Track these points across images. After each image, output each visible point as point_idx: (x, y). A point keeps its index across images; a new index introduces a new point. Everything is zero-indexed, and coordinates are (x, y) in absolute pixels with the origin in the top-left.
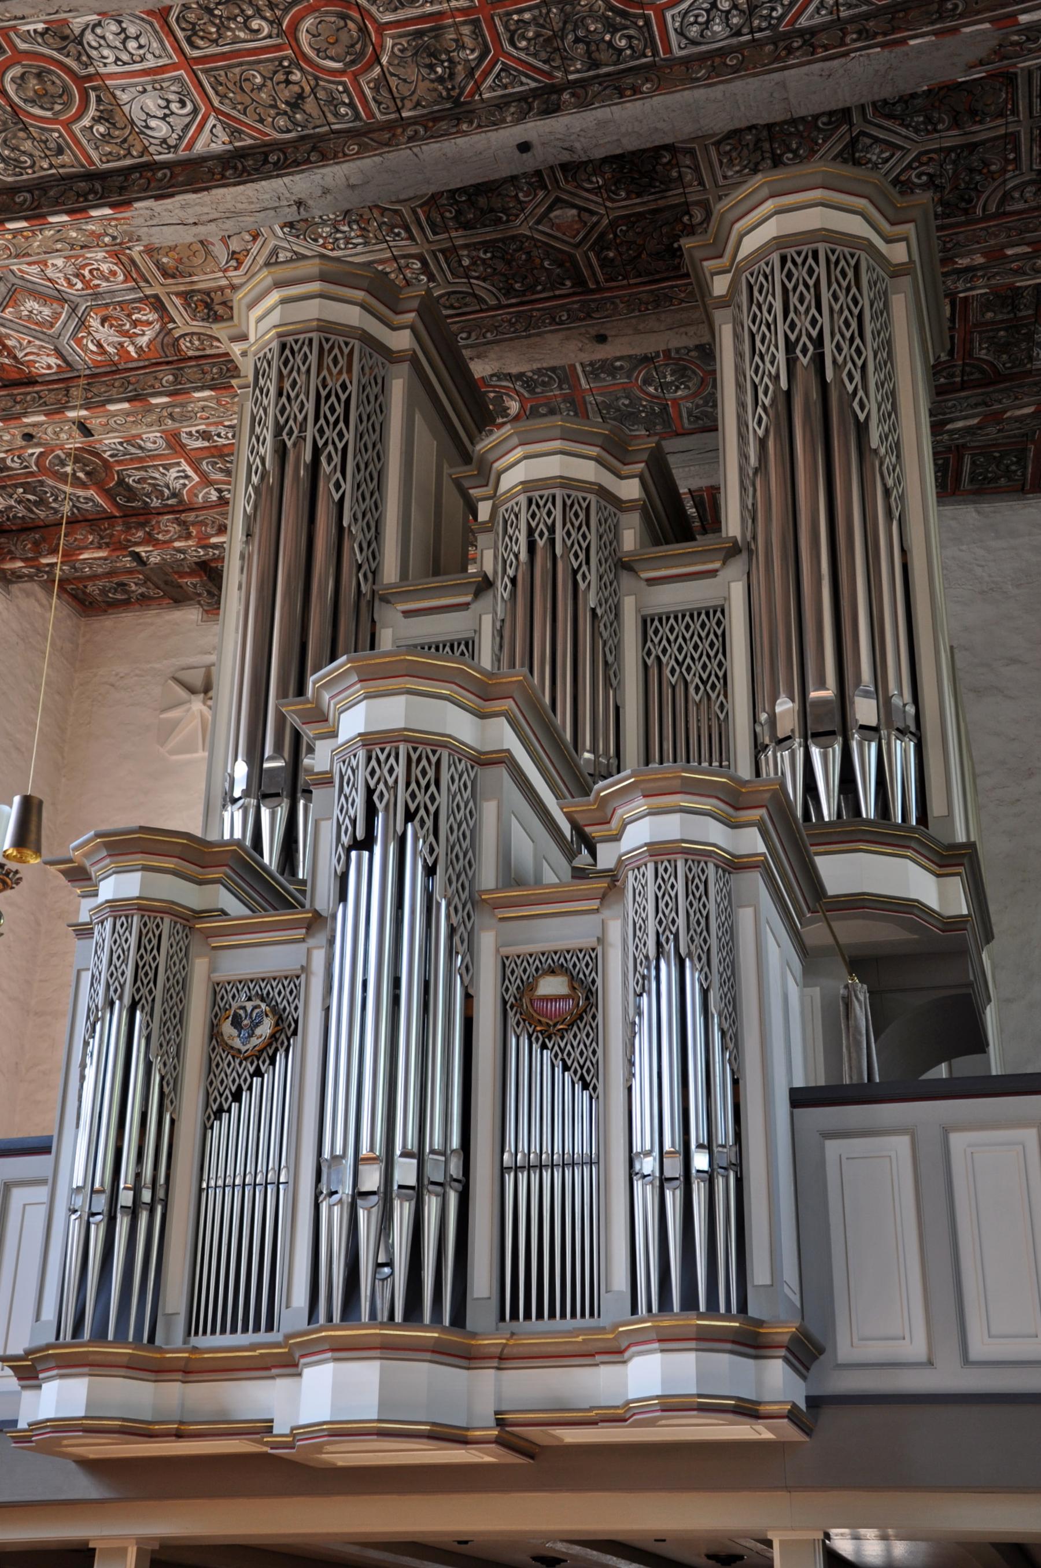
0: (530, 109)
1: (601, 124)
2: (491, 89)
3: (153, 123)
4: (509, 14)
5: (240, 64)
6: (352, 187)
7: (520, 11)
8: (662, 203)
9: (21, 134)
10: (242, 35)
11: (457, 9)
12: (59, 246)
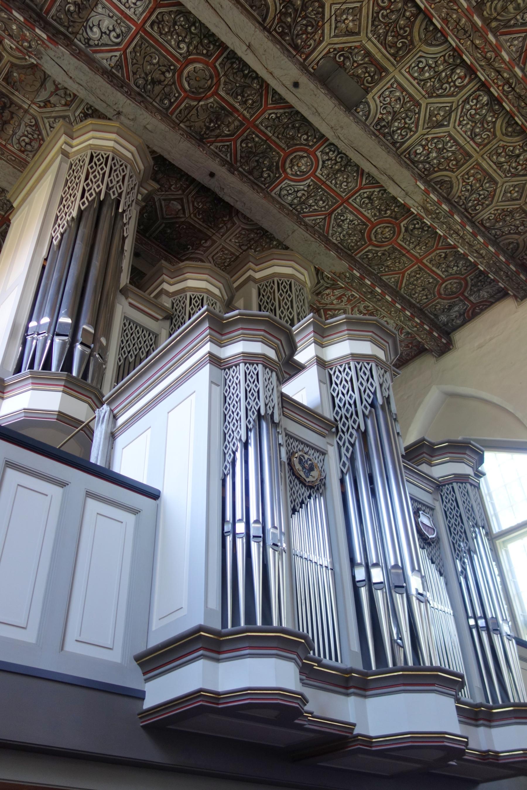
4: (254, 133)
5: (157, 50)
6: (145, 127)
7: (257, 136)
8: (205, 230)
11: (244, 115)
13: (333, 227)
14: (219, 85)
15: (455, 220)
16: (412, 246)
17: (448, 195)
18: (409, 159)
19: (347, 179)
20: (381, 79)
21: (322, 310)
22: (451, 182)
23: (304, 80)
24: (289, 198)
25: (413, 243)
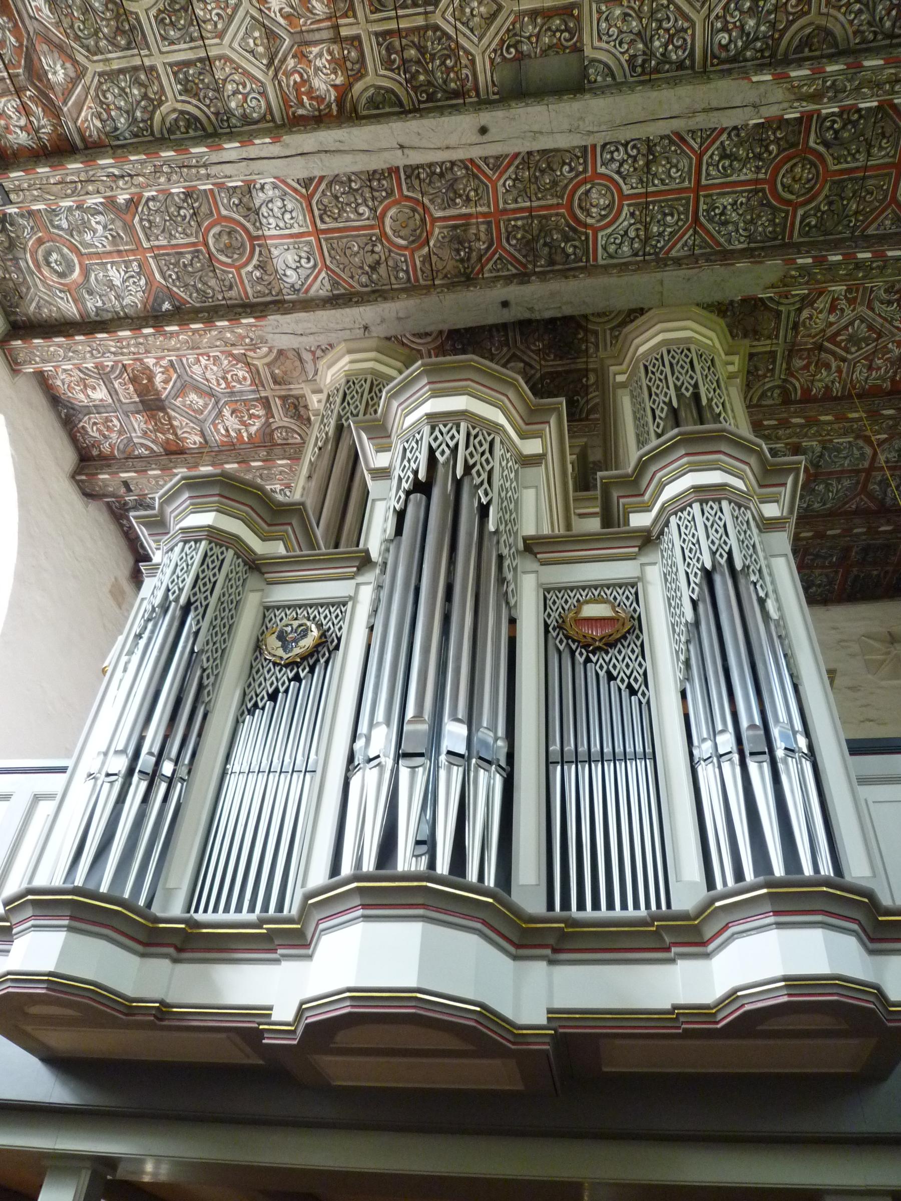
1: (552, 295)
2: (490, 271)
3: (289, 272)
4: (509, 220)
5: (347, 237)
6: (399, 319)
7: (516, 219)
8: (573, 366)
9: (211, 274)
10: (352, 216)
12: (218, 343)
13: (719, 232)
14: (428, 209)
15: (873, 69)
16: (861, 157)
17: (836, 45)
19: (668, 163)
20: (578, 19)
21: (826, 344)
22: (818, 28)
23: (485, 117)
24: (625, 249)
25: (858, 151)
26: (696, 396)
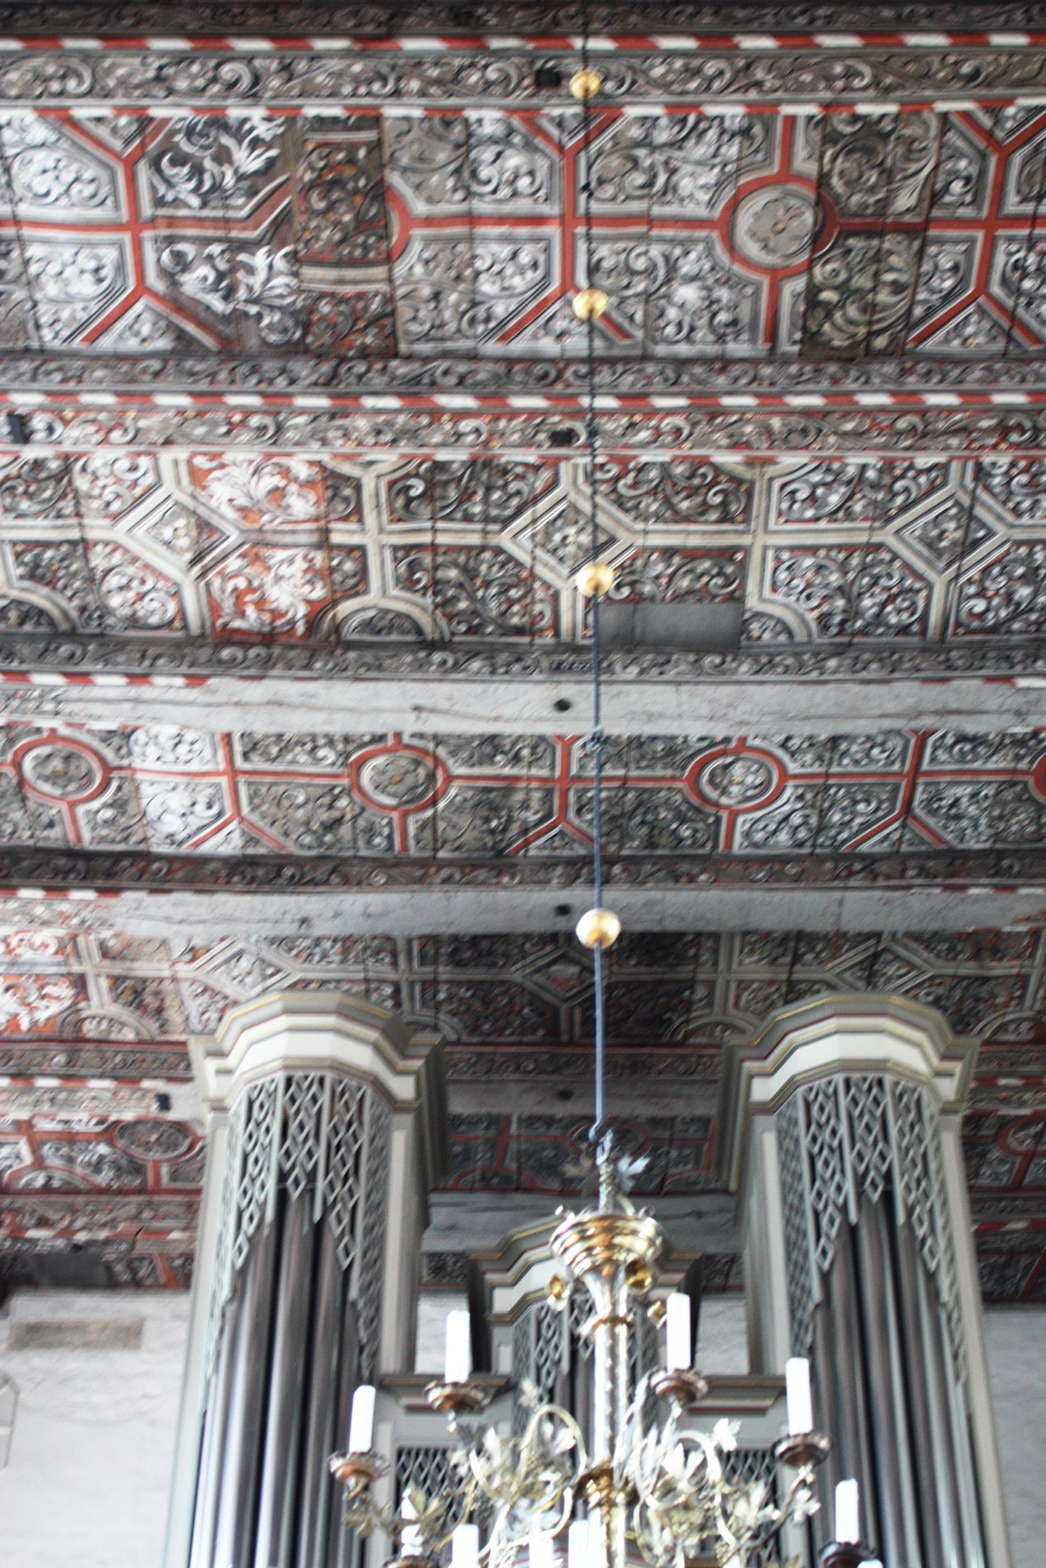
0: (577, 877)
1: (649, 904)
2: (539, 848)
8: (668, 976)
18: (970, 632)
20: (743, 565)
23: (567, 690)
26: (888, 1197)
